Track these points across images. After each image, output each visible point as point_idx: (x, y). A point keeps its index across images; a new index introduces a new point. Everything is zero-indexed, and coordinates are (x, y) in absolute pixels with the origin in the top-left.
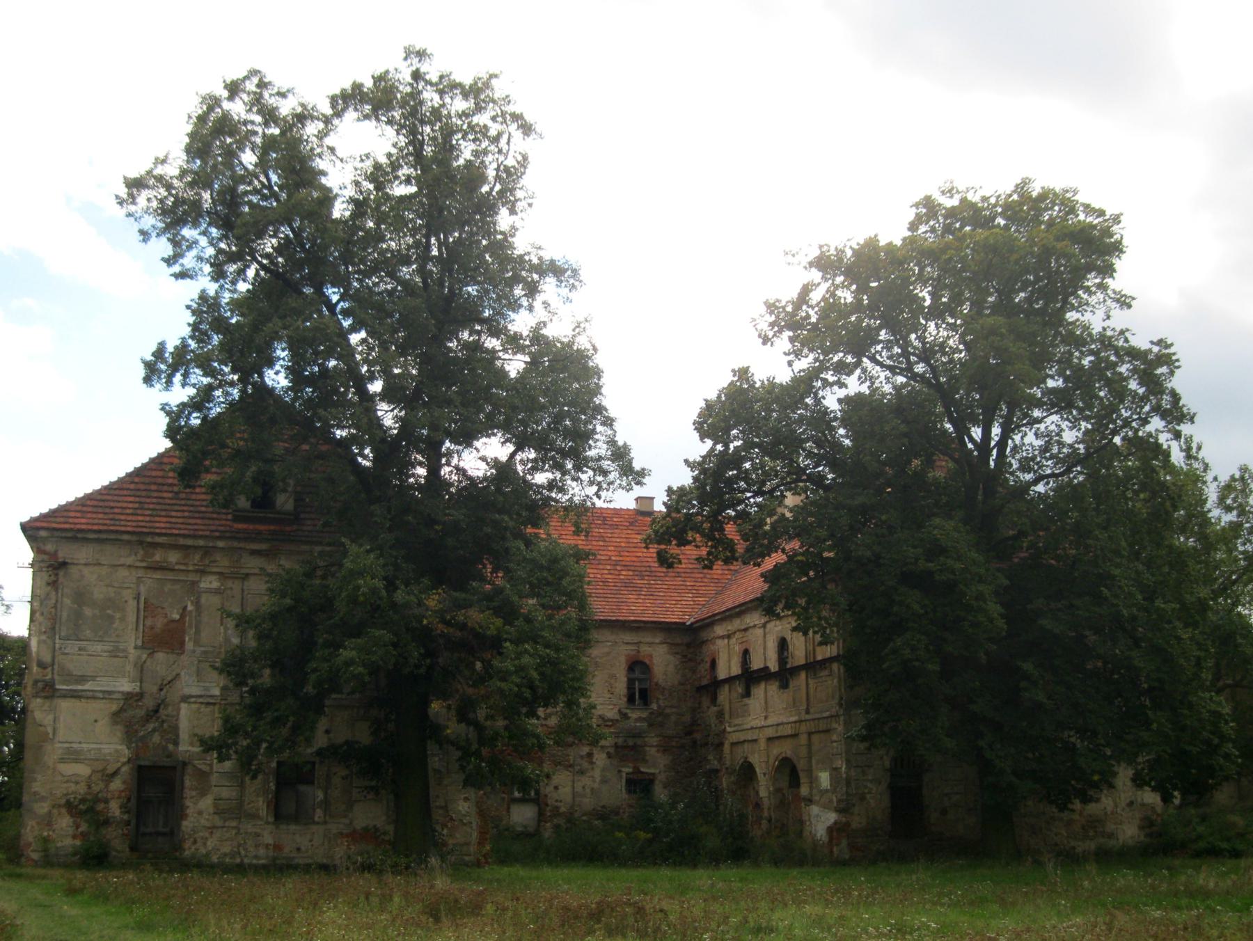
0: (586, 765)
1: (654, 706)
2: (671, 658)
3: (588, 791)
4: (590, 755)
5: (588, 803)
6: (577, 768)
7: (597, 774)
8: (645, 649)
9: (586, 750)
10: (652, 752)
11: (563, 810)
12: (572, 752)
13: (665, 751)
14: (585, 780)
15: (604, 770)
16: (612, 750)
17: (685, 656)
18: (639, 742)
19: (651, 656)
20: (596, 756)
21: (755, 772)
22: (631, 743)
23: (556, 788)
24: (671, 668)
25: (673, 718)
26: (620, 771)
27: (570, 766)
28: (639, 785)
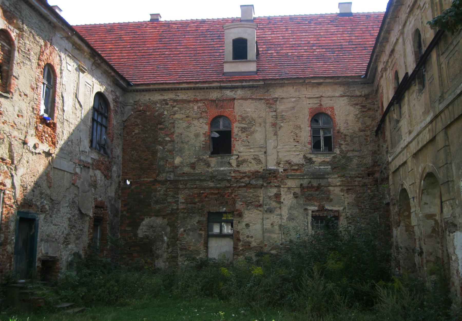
0: (274, 204)
1: (337, 151)
2: (352, 108)
3: (277, 227)
4: (278, 196)
5: (277, 237)
6: (266, 208)
7: (285, 212)
8: (326, 103)
9: (274, 191)
10: (336, 191)
11: (254, 244)
12: (261, 193)
14: (274, 218)
15: (291, 208)
16: (298, 191)
17: (364, 107)
18: (323, 182)
19: (332, 108)
20: (283, 197)
21: (407, 195)
22: (315, 183)
23: (247, 225)
24: (351, 117)
25: (355, 161)
26: (306, 209)
27: (260, 206)
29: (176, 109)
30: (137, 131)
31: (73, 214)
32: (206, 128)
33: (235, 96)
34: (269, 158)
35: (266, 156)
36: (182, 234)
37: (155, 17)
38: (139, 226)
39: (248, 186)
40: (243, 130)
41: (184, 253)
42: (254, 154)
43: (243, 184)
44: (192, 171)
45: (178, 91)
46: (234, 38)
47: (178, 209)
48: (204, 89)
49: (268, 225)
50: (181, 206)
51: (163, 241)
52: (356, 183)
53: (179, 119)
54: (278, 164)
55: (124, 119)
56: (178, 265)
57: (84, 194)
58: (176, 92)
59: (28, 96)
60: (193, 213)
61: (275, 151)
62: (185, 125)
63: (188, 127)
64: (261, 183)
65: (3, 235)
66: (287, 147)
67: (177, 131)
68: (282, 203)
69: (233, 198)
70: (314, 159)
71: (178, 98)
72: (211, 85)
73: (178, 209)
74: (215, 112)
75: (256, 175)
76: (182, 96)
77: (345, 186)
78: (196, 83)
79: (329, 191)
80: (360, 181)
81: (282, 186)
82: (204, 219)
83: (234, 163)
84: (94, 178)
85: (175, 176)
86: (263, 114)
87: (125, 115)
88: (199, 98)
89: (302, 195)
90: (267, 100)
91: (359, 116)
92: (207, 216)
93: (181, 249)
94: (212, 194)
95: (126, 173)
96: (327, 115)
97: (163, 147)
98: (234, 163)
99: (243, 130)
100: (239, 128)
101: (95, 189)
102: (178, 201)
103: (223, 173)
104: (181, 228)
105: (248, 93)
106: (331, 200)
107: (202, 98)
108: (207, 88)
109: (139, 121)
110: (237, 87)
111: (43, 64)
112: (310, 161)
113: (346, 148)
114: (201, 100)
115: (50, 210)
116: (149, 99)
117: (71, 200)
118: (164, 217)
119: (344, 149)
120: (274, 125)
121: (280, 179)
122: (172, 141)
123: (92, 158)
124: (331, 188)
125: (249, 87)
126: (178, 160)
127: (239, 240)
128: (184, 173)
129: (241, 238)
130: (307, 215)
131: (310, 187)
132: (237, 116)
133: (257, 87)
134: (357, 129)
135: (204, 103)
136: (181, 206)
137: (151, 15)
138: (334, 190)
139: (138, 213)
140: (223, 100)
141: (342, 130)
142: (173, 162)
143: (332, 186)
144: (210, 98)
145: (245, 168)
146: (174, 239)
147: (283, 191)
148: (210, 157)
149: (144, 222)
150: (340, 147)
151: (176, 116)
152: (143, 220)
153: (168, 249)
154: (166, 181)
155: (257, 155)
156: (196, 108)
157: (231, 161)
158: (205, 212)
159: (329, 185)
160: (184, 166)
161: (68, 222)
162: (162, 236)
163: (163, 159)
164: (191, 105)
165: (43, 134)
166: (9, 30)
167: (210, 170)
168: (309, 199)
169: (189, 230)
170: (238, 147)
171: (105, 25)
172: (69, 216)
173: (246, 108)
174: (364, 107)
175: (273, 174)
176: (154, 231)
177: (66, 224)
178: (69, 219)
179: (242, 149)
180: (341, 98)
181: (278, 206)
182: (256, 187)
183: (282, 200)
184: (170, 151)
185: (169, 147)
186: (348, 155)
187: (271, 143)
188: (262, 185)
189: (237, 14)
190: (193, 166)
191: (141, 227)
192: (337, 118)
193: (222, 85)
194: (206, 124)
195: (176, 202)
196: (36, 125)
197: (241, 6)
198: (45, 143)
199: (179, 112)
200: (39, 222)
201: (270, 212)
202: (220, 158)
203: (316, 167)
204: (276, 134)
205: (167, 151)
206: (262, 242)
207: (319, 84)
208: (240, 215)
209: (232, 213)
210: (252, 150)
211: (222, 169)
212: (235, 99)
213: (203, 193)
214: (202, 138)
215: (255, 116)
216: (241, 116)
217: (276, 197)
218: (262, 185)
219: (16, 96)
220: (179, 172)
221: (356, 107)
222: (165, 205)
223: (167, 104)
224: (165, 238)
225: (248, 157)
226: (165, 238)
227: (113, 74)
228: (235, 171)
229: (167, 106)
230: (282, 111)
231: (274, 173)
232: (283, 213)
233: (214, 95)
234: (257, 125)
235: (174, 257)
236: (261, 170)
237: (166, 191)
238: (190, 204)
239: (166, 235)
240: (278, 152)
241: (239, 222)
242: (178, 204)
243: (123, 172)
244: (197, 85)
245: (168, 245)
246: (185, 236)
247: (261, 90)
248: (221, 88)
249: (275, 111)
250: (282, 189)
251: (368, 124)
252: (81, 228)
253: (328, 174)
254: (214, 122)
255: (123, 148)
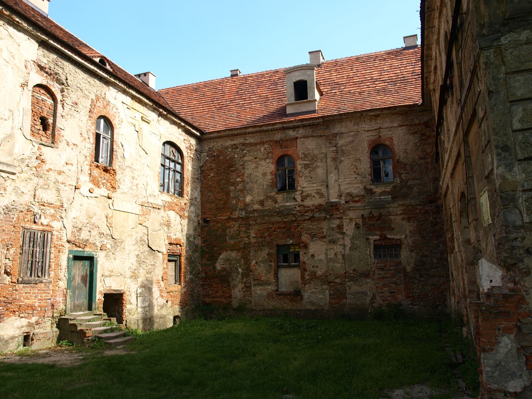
2: (411, 137)
3: (340, 257)
4: (340, 227)
8: (385, 134)
9: (337, 222)
10: (397, 220)
11: (319, 273)
12: (325, 225)
13: (409, 219)
14: (338, 248)
15: (353, 238)
16: (360, 221)
18: (383, 212)
19: (391, 139)
20: (345, 228)
22: (376, 213)
23: (313, 256)
26: (367, 239)
27: (324, 237)
28: (386, 249)
29: (245, 151)
30: (212, 175)
31: (142, 251)
32: (272, 168)
33: (297, 136)
34: (331, 191)
35: (328, 190)
36: (254, 266)
37: (235, 73)
38: (217, 260)
39: (312, 219)
40: (306, 166)
41: (256, 283)
42: (316, 188)
43: (308, 218)
44: (261, 208)
45: (246, 136)
46: (295, 81)
47: (250, 243)
48: (268, 131)
49: (331, 255)
50: (253, 240)
51: (238, 273)
52: (418, 211)
53: (248, 161)
54: (340, 196)
55: (201, 165)
56: (251, 294)
57: (155, 233)
58: (244, 136)
59: (78, 145)
60: (263, 246)
61: (336, 185)
62: (253, 166)
63: (257, 168)
64: (324, 215)
65: (53, 272)
66: (348, 179)
67: (247, 172)
68: (345, 233)
69: (298, 231)
70: (375, 190)
71: (247, 142)
72: (274, 127)
73: (250, 243)
74: (279, 152)
75: (319, 208)
76: (250, 140)
77: (406, 214)
78: (261, 126)
79: (391, 220)
80: (421, 209)
81: (344, 217)
82: (274, 251)
83: (299, 199)
84: (167, 218)
85: (246, 213)
86: (324, 150)
87: (201, 160)
88: (264, 140)
89: (363, 225)
90: (328, 136)
91: (418, 144)
92: (276, 249)
93: (254, 280)
94: (280, 228)
95: (205, 213)
96: (386, 146)
97: (235, 188)
98: (299, 199)
99: (306, 166)
100: (302, 165)
101: (168, 228)
102: (250, 236)
103: (290, 209)
104: (253, 260)
105: (309, 131)
106: (393, 229)
107: (268, 139)
108: (271, 130)
109: (213, 165)
110: (298, 127)
111: (95, 116)
112: (370, 192)
113: (406, 177)
114: (267, 142)
115: (112, 248)
116: (222, 145)
117: (139, 239)
118: (238, 250)
119: (404, 178)
120: (334, 159)
121: (342, 211)
122: (243, 181)
123: (163, 201)
124: (392, 218)
125: (309, 125)
126: (248, 199)
127: (305, 270)
128: (254, 210)
129: (307, 267)
130: (369, 244)
131: (371, 217)
132: (300, 154)
133: (318, 124)
134: (417, 157)
135: (270, 144)
136: (253, 240)
137: (231, 71)
138: (396, 219)
139: (215, 249)
140: (287, 140)
141: (401, 160)
142: (244, 200)
143: (393, 215)
144: (274, 140)
145: (309, 202)
146: (248, 272)
147: (345, 222)
148: (277, 193)
149: (221, 256)
150: (400, 176)
151: (246, 158)
152: (220, 254)
153: (242, 279)
154: (239, 218)
155: (320, 189)
156: (263, 149)
157: (296, 196)
158: (274, 245)
159: (390, 214)
160: (254, 203)
161: (136, 258)
162: (237, 268)
163: (235, 198)
164: (258, 147)
165: (100, 179)
166: (48, 86)
167: (277, 206)
168: (370, 229)
169: (260, 261)
170: (303, 184)
171: (193, 85)
172: (137, 253)
173: (308, 145)
174: (423, 135)
175: (335, 206)
176: (230, 264)
177: (134, 260)
178: (138, 255)
179: (305, 185)
180: (399, 128)
181: (341, 236)
182: (319, 220)
183: (344, 231)
184: (242, 191)
185: (239, 187)
186: (408, 184)
187: (333, 177)
188: (326, 218)
189: (306, 60)
190: (262, 203)
191: (219, 261)
192: (396, 148)
193: (284, 125)
194: (272, 163)
195: (248, 237)
196: (89, 172)
197: (309, 53)
198: (103, 188)
199: (248, 155)
200: (98, 259)
201: (334, 242)
202: (285, 194)
203: (376, 197)
204: (337, 168)
205: (238, 191)
206: (326, 272)
207: (377, 116)
208: (306, 246)
209: (298, 244)
210: (315, 185)
211: (288, 204)
212: (297, 138)
213: (271, 228)
214: (269, 177)
215: (316, 152)
216: (304, 153)
217: (339, 229)
218: (326, 218)
219: (62, 145)
220: (249, 209)
221: (416, 135)
222: (238, 240)
223: (237, 148)
224: (240, 270)
225: (311, 192)
226: (240, 270)
227: (183, 124)
228: (299, 206)
229: (237, 150)
230: (342, 146)
231: (335, 206)
232: (346, 243)
233: (278, 136)
234: (319, 160)
235: (247, 287)
236: (324, 203)
237: (239, 227)
238: (261, 238)
239: (240, 266)
240: (339, 185)
241: (305, 253)
242: (249, 239)
243: (202, 212)
244: (262, 128)
245: (242, 276)
246: (257, 267)
247: (321, 127)
248: (284, 129)
249: (335, 146)
250: (344, 221)
251: (428, 151)
252: (153, 263)
253: (388, 203)
254: (280, 161)
255: (201, 191)
